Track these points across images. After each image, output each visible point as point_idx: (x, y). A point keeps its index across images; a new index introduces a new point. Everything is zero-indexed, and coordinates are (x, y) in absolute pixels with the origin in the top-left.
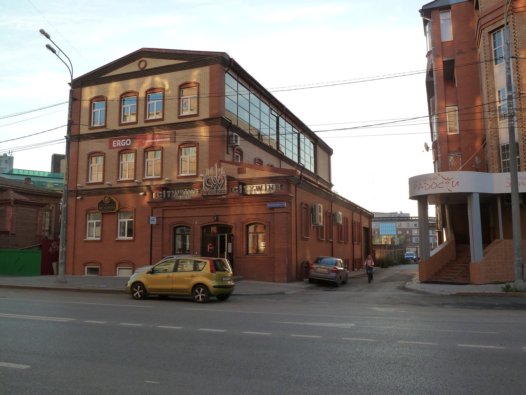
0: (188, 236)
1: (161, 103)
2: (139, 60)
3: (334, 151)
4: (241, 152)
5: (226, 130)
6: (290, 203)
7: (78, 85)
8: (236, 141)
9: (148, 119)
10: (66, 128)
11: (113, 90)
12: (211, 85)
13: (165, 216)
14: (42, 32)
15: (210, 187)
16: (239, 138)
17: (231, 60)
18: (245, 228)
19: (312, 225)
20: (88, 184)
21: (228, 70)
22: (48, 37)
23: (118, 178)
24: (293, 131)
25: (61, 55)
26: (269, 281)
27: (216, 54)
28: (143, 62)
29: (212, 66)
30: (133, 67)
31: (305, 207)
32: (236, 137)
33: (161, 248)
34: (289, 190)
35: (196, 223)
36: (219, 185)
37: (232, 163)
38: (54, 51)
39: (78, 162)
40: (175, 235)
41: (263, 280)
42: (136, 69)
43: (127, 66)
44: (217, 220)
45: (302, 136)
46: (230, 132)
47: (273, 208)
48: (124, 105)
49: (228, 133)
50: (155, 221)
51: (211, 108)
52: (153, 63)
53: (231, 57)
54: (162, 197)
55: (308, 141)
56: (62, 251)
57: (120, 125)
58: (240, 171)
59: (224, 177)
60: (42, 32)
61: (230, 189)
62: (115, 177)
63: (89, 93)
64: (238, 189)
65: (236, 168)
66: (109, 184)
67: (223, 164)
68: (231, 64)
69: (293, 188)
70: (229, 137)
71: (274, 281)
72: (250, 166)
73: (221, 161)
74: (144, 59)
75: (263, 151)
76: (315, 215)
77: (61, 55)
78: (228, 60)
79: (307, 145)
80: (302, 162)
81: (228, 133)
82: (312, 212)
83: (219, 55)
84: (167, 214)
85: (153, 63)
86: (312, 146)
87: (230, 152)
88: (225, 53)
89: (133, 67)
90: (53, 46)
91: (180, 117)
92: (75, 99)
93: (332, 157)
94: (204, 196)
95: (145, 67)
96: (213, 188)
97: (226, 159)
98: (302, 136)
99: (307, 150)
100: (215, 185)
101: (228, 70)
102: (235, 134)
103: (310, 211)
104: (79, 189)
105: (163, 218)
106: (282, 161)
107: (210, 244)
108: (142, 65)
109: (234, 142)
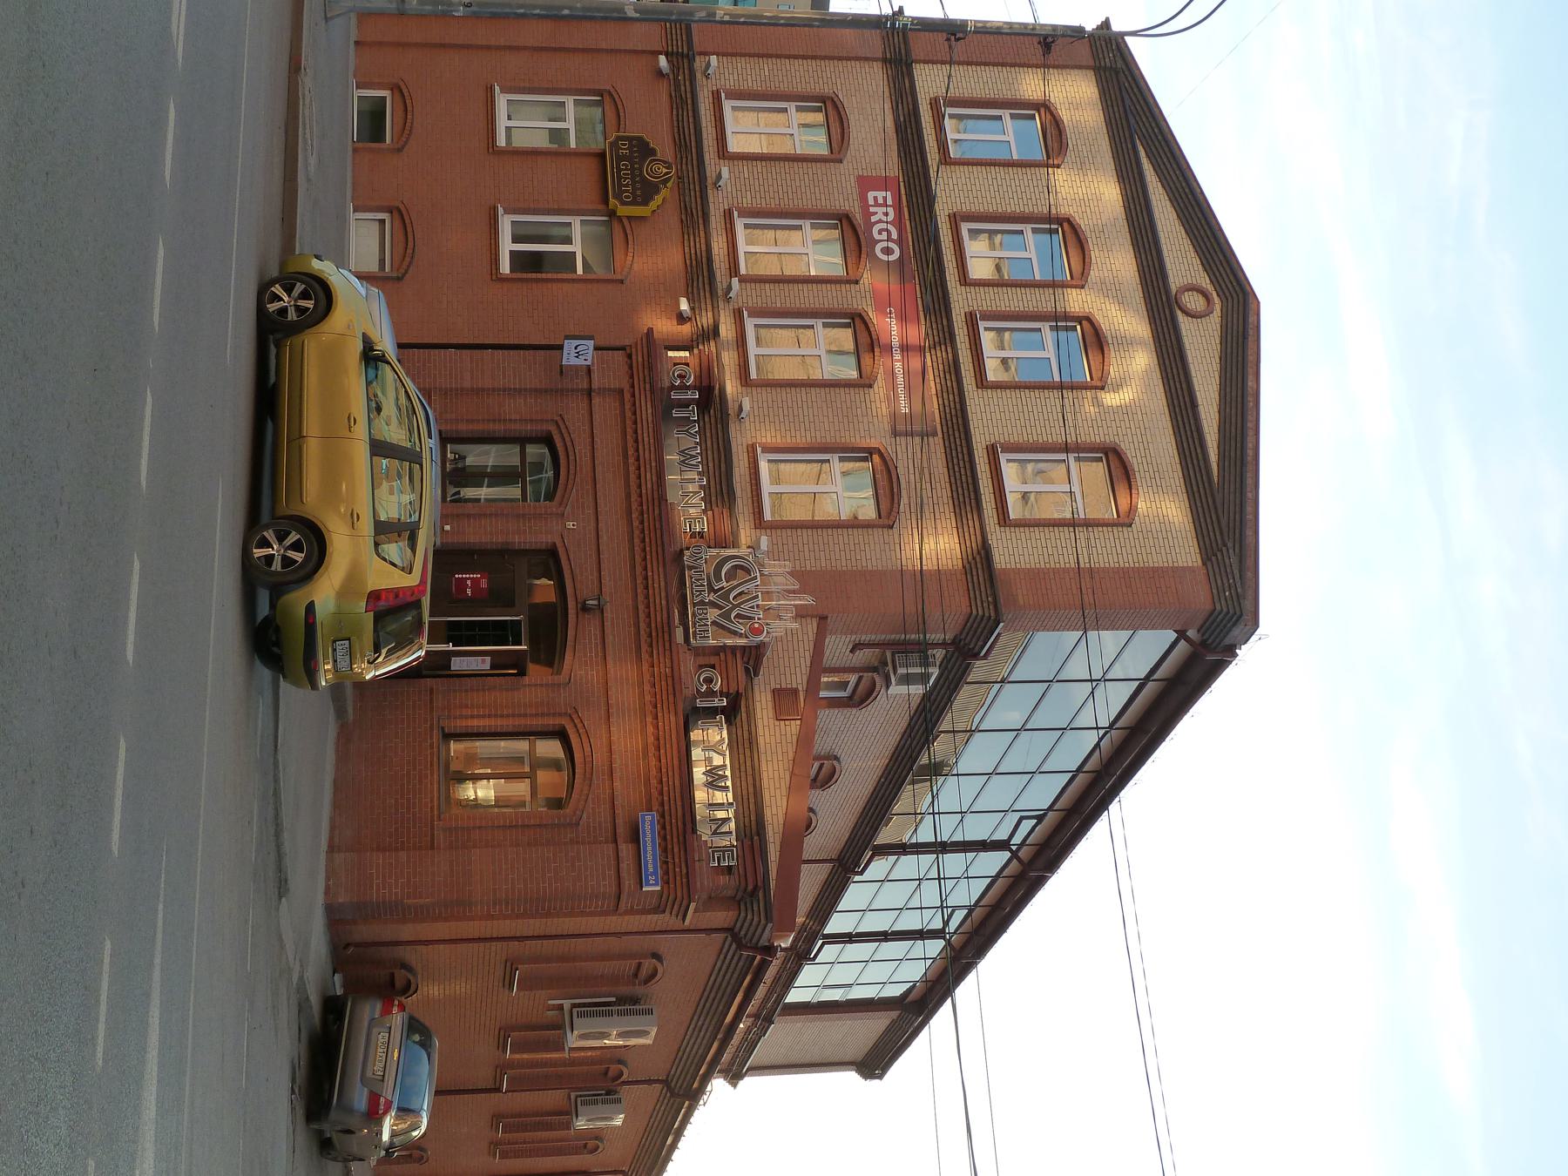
0: (514, 492)
1: (1046, 378)
2: (1210, 288)
4: (860, 699)
5: (949, 637)
8: (907, 680)
9: (982, 325)
10: (937, 14)
11: (1090, 191)
12: (1124, 574)
13: (596, 401)
15: (719, 579)
16: (917, 690)
17: (1230, 652)
18: (552, 722)
19: (567, 1004)
20: (716, 97)
21: (1188, 640)
23: (745, 213)
24: (954, 909)
26: (332, 828)
27: (1250, 593)
30: (1182, 264)
31: (644, 973)
32: (924, 678)
33: (467, 384)
34: (712, 901)
35: (570, 525)
36: (726, 616)
37: (817, 667)
39: (804, 57)
40: (522, 441)
41: (336, 805)
42: (1175, 280)
43: (1187, 242)
44: (585, 609)
45: (935, 947)
46: (939, 654)
47: (635, 837)
49: (936, 645)
50: (574, 361)
51: (1037, 576)
52: (1201, 342)
53: (1243, 652)
54: (673, 387)
55: (914, 972)
57: (955, 220)
59: (758, 632)
61: (713, 660)
62: (747, 202)
63: (1075, 96)
64: (711, 693)
65: (799, 680)
66: (719, 177)
67: (812, 626)
69: (721, 917)
70: (920, 650)
71: (332, 848)
72: (805, 740)
73: (823, 619)
74: (1218, 307)
75: (871, 788)
76: (610, 1014)
78: (1227, 641)
79: (899, 971)
80: (830, 952)
81: (936, 645)
82: (621, 1000)
83: (1247, 604)
84: (605, 409)
85: (1201, 342)
86: (895, 991)
87: (863, 656)
88: (1256, 625)
89: (1182, 264)
92: (1048, 46)
93: (851, 1077)
94: (682, 551)
95: (1183, 311)
97: (830, 641)
98: (935, 947)
99: (878, 972)
100: (725, 596)
101: (1188, 640)
102: (935, 672)
103: (624, 990)
104: (699, 62)
105: (589, 393)
106: (830, 866)
107: (484, 584)
108: (1193, 301)
109: (902, 671)
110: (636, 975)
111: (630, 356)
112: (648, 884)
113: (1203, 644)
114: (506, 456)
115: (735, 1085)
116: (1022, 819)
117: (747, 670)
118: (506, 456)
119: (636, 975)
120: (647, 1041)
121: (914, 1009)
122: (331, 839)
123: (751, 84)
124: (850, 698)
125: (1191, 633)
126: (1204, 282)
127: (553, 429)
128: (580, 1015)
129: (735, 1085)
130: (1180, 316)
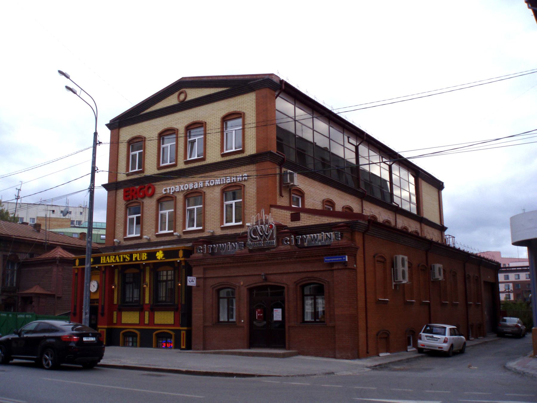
0: (234, 300)
1: (203, 140)
3: (444, 184)
4: (301, 193)
5: (278, 166)
6: (355, 256)
7: (117, 124)
8: (292, 179)
9: (188, 159)
10: (90, 175)
11: (149, 129)
12: (258, 114)
13: (207, 276)
14: (60, 72)
15: (256, 238)
16: (296, 175)
17: (282, 81)
19: (394, 283)
20: (126, 240)
22: (68, 77)
23: (157, 230)
25: (83, 95)
27: (263, 76)
28: (189, 94)
29: (258, 91)
30: (172, 100)
31: (382, 260)
33: (202, 315)
34: (353, 240)
35: (242, 283)
36: (267, 236)
38: (75, 93)
39: (115, 214)
40: (219, 298)
41: (323, 356)
44: (266, 279)
46: (284, 170)
47: (332, 264)
48: (163, 144)
50: (195, 282)
52: (193, 94)
53: (282, 78)
54: (203, 253)
56: (86, 319)
57: (159, 168)
58: (295, 217)
59: (271, 226)
60: (60, 72)
61: (280, 239)
62: (154, 230)
63: (127, 133)
64: (203, 249)
65: (288, 213)
66: (146, 239)
67: (273, 210)
68: (281, 86)
69: (358, 238)
70: (282, 176)
71: (335, 357)
73: (272, 206)
76: (396, 270)
77: (83, 95)
83: (266, 77)
84: (210, 274)
85: (193, 94)
87: (286, 195)
88: (272, 74)
89: (172, 100)
90: (72, 86)
91: (223, 155)
93: (443, 192)
94: (249, 250)
96: (260, 240)
97: (279, 203)
100: (261, 236)
102: (289, 171)
104: (116, 244)
105: (205, 278)
107: (259, 310)
108: (182, 97)
110: (383, 262)
111: (194, 266)
112: (345, 260)
113: (281, 89)
114: (224, 304)
115: (446, 228)
116: (349, 142)
117: (285, 229)
118: (224, 304)
119: (383, 262)
120: (406, 258)
121: (418, 173)
122: (332, 357)
123: (122, 229)
124: (301, 197)
125: (277, 93)
126: (176, 94)
127: (215, 289)
128: (397, 279)
129: (446, 228)
130: (187, 100)
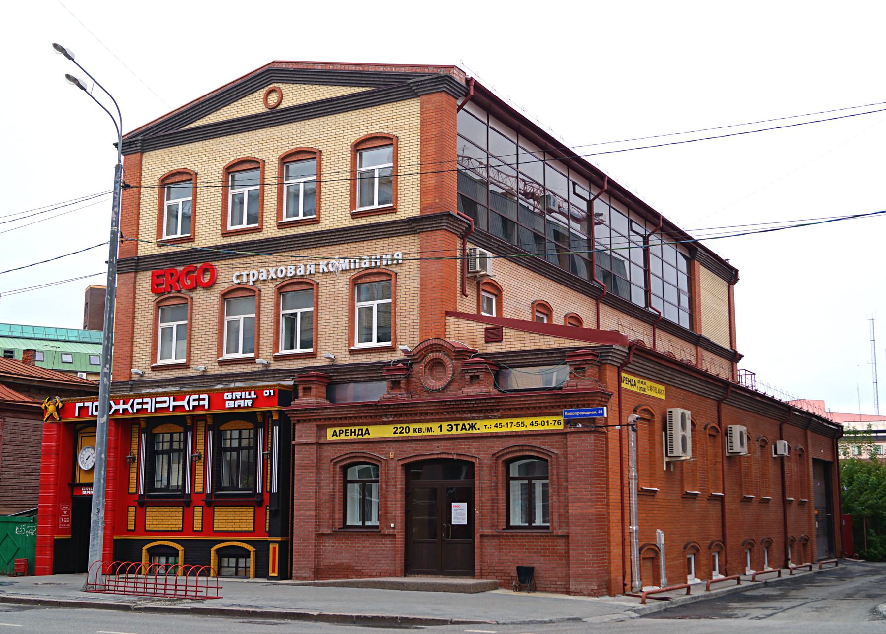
0: (374, 487)
2: (266, 89)
3: (740, 274)
4: (497, 290)
8: (484, 266)
11: (207, 159)
12: (424, 142)
18: (501, 468)
21: (463, 104)
24: (631, 229)
25: (97, 93)
26: (556, 592)
28: (279, 91)
31: (647, 416)
32: (483, 257)
34: (601, 379)
37: (476, 318)
39: (134, 318)
40: (345, 482)
42: (260, 109)
43: (240, 102)
45: (654, 240)
46: (469, 246)
49: (464, 249)
51: (423, 192)
52: (295, 95)
55: (670, 252)
57: (226, 234)
58: (494, 335)
60: (55, 46)
63: (157, 163)
69: (610, 374)
70: (466, 259)
71: (568, 593)
72: (518, 325)
73: (448, 313)
74: (276, 85)
75: (552, 282)
76: (671, 435)
77: (97, 93)
78: (463, 83)
79: (669, 260)
80: (656, 303)
81: (464, 249)
82: (665, 429)
85: (295, 95)
86: (683, 264)
87: (471, 291)
92: (126, 186)
93: (737, 287)
95: (279, 105)
97: (460, 309)
98: (654, 240)
99: (670, 274)
101: (463, 104)
102: (479, 250)
103: (658, 425)
104: (135, 378)
106: (601, 306)
108: (273, 99)
109: (478, 269)
110: (648, 420)
111: (299, 421)
113: (467, 94)
114: (354, 493)
115: (741, 357)
116: (575, 193)
117: (474, 357)
118: (354, 493)
119: (648, 420)
120: (688, 413)
121: (693, 251)
122: (562, 592)
123: (148, 350)
124: (496, 296)
125: (459, 103)
126: (263, 92)
127: (338, 466)
128: (672, 452)
129: (741, 357)
130: (282, 106)
